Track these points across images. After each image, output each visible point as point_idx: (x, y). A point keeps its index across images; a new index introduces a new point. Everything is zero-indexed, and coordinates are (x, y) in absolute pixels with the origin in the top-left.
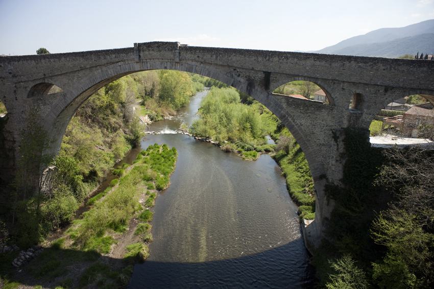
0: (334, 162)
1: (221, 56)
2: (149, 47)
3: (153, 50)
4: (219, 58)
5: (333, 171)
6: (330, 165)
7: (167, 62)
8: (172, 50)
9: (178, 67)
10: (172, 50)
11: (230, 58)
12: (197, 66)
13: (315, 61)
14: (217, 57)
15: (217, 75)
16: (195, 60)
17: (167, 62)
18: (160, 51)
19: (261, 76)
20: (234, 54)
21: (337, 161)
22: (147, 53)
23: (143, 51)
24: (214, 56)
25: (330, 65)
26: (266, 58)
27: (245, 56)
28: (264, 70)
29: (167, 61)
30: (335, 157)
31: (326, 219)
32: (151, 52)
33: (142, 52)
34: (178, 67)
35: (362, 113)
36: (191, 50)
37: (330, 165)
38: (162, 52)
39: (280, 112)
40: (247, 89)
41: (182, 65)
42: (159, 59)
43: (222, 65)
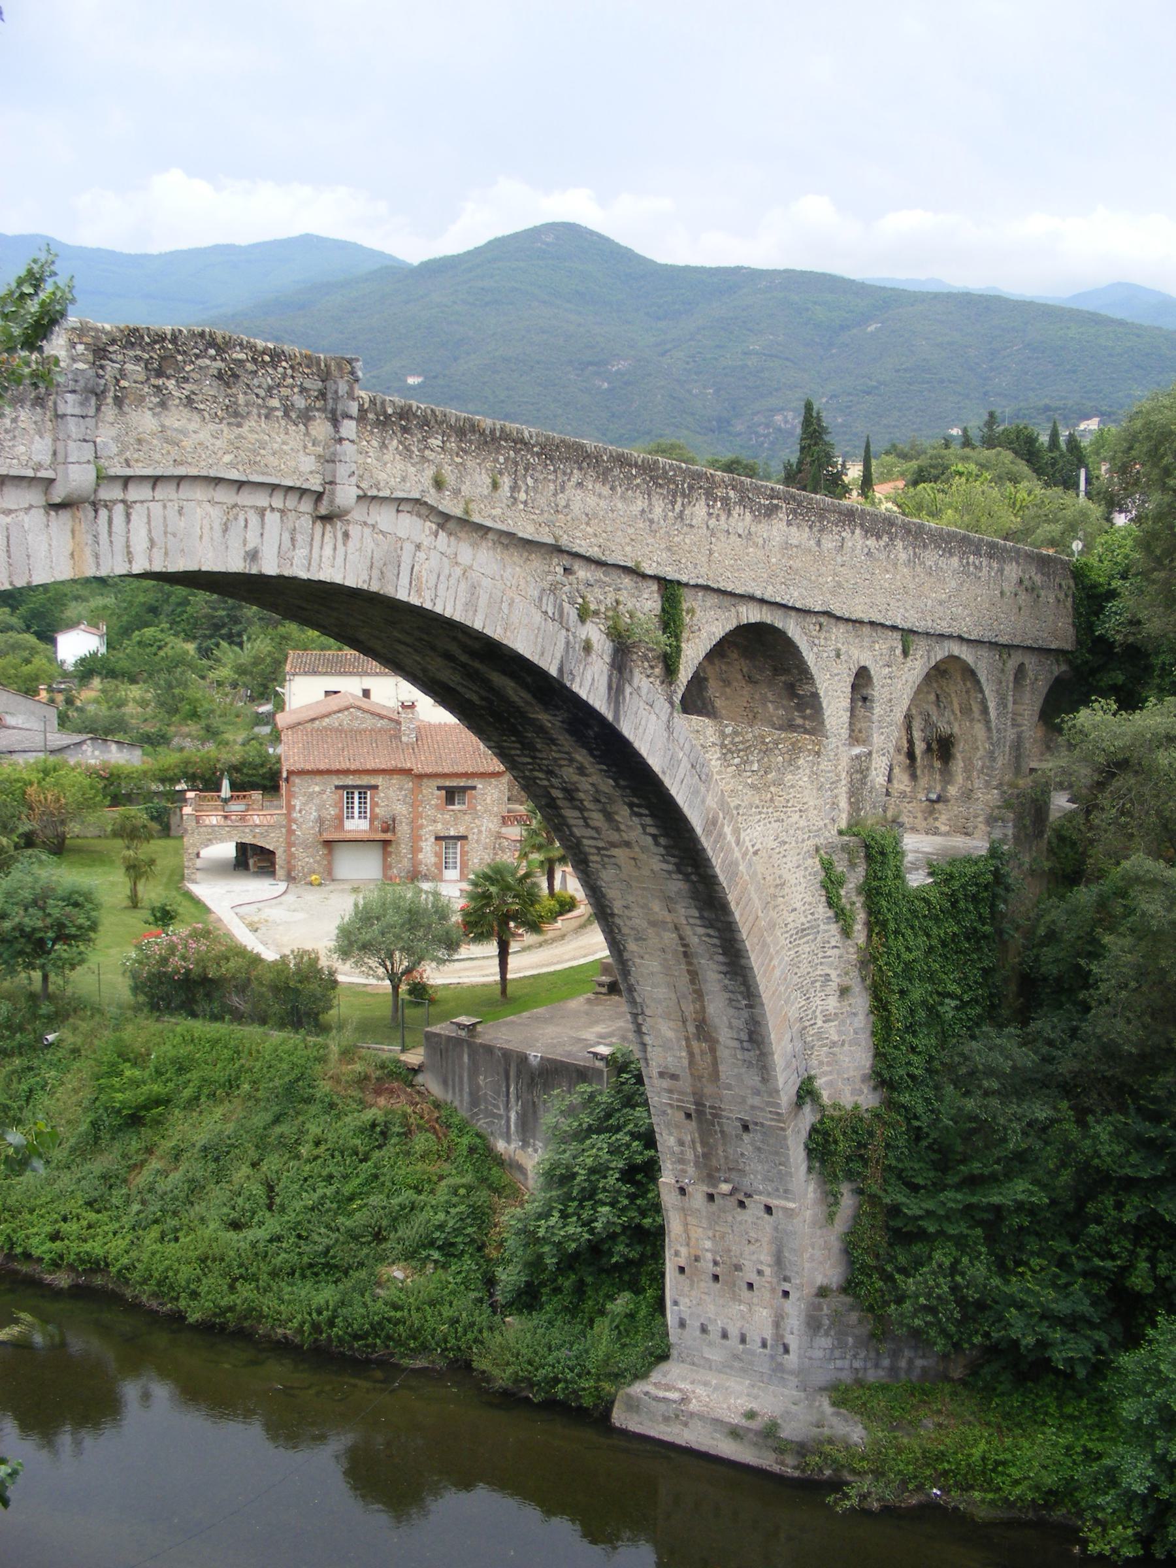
0: (832, 1003)
1: (530, 481)
2: (160, 373)
3: (189, 401)
4: (522, 496)
5: (834, 1044)
6: (820, 1023)
7: (261, 512)
8: (305, 417)
9: (328, 551)
10: (305, 417)
11: (562, 500)
12: (418, 547)
13: (789, 524)
14: (515, 488)
15: (505, 606)
16: (418, 505)
17: (261, 512)
18: (235, 415)
19: (649, 603)
20: (577, 476)
21: (844, 991)
22: (145, 420)
23: (119, 402)
24: (506, 481)
25: (819, 543)
26: (673, 503)
27: (613, 488)
28: (671, 573)
29: (261, 499)
30: (834, 974)
31: (823, 1292)
32: (177, 418)
33: (109, 411)
34: (328, 551)
35: (870, 753)
36: (405, 430)
37: (820, 1023)
38: (253, 429)
39: (703, 802)
40: (610, 688)
41: (346, 535)
42: (217, 481)
43: (528, 545)
